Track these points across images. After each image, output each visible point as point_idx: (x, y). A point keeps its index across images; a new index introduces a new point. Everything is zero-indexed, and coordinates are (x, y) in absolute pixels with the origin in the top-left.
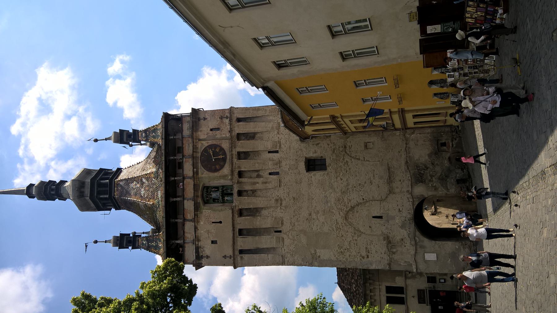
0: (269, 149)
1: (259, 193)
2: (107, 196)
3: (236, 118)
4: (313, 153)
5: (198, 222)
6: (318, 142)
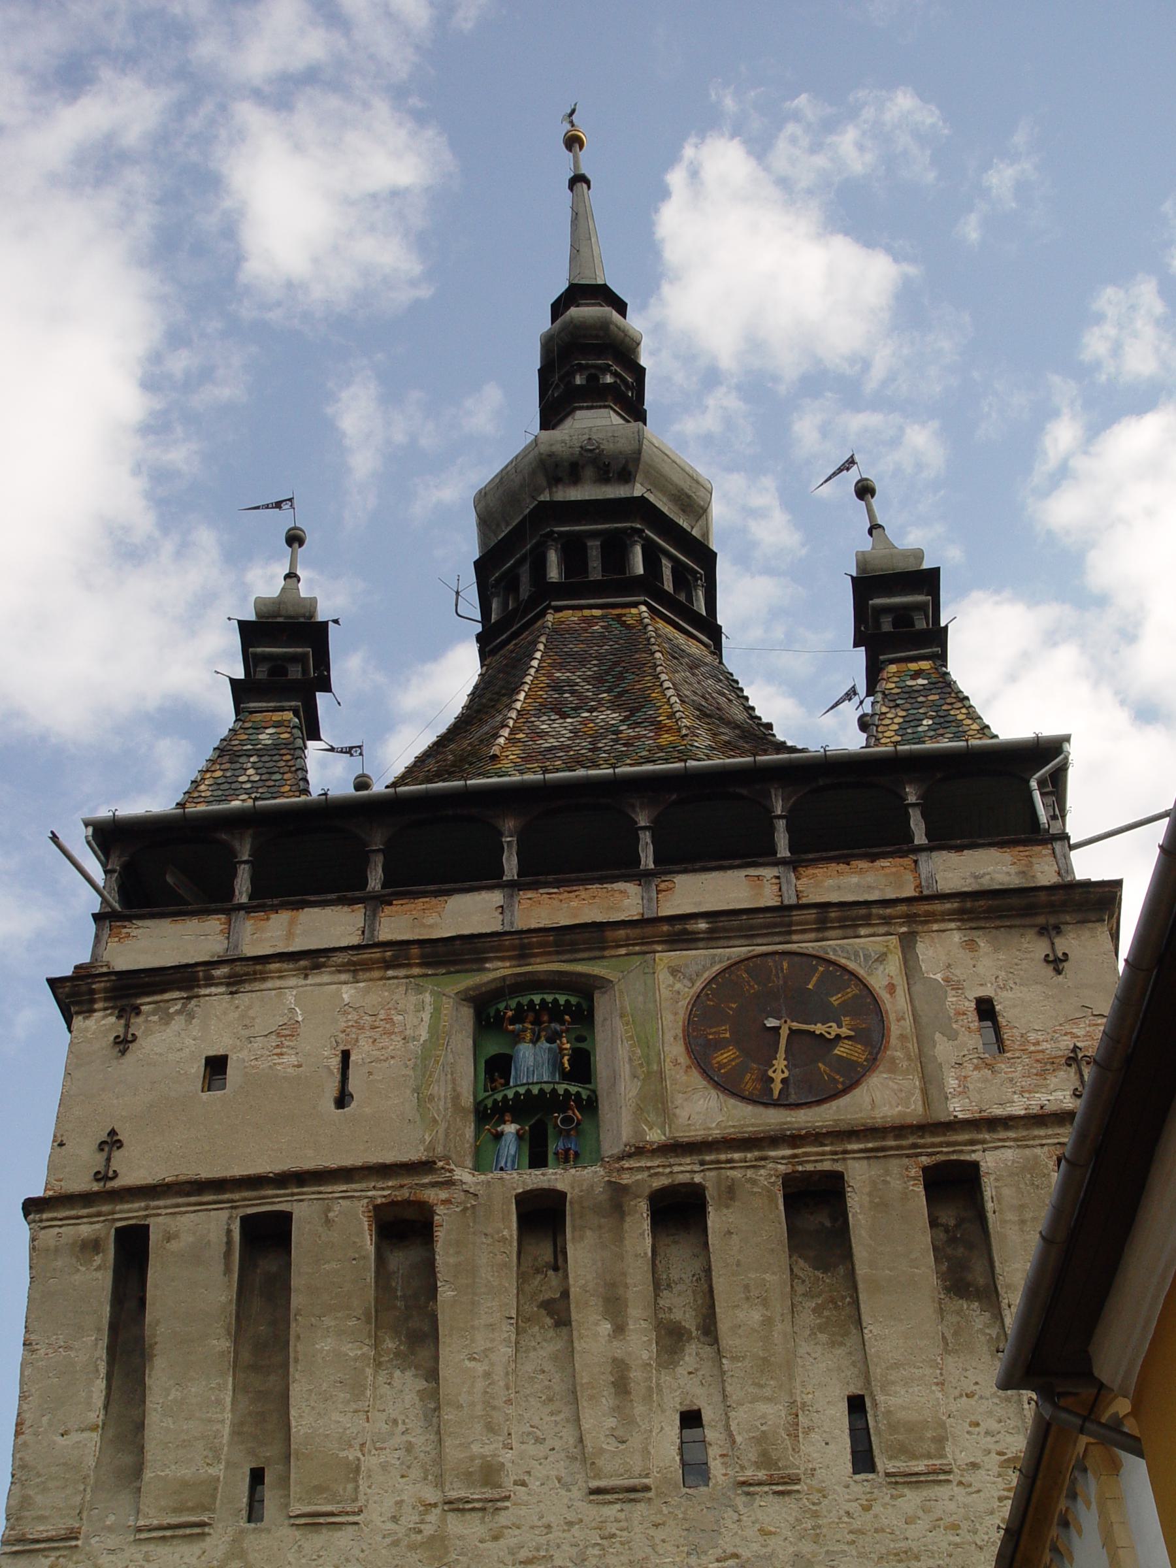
0: (880, 1398)
2: (554, 573)
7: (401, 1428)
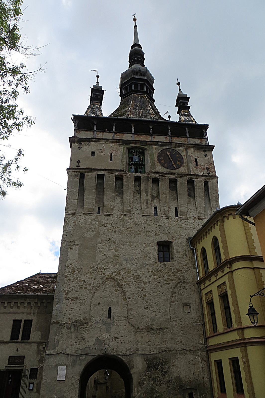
0: (180, 208)
1: (137, 197)
3: (208, 180)
4: (177, 250)
5: (112, 143)
6: (188, 255)
7: (118, 204)
